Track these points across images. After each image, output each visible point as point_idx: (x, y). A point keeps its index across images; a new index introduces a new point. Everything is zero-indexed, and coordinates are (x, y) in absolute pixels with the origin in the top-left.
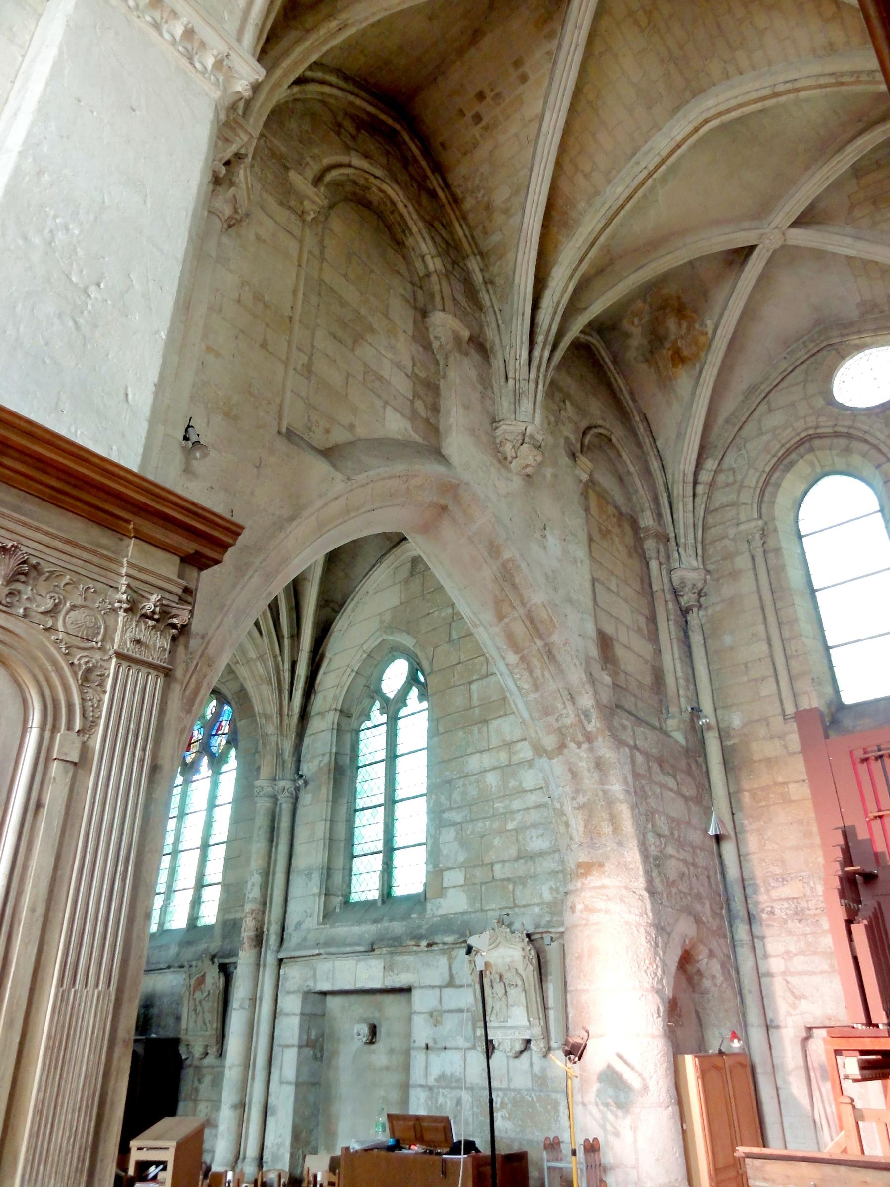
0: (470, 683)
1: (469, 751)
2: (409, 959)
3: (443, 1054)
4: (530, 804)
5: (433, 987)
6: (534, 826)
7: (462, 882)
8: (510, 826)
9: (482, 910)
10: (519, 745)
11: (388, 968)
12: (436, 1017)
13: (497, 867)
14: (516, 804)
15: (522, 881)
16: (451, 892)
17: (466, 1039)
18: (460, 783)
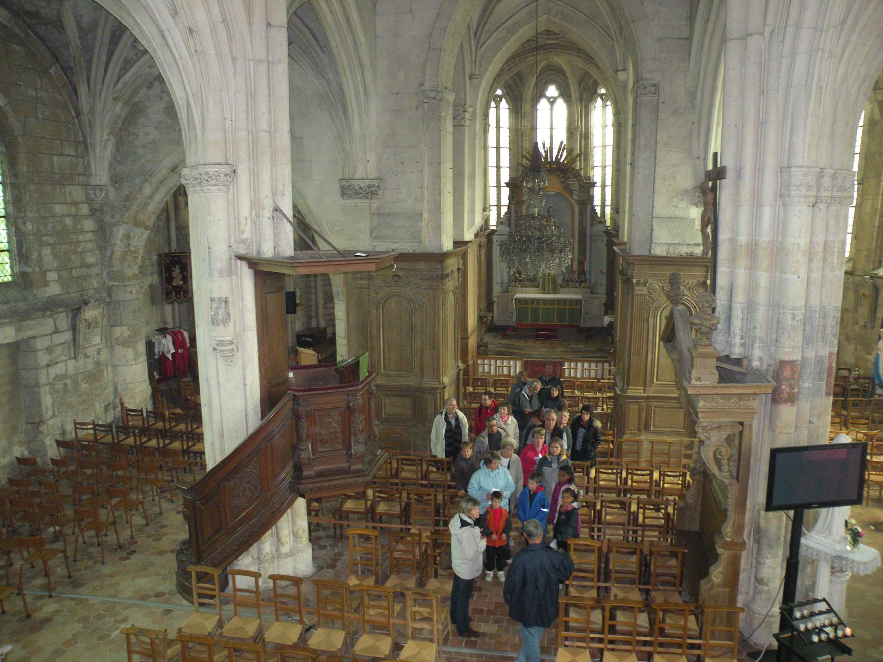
0: (53, 155)
1: (55, 201)
2: (31, 322)
3: (56, 366)
4: (87, 239)
5: (47, 335)
6: (90, 250)
7: (57, 278)
8: (79, 249)
9: (68, 293)
10: (81, 205)
11: (19, 330)
12: (49, 350)
13: (74, 270)
14: (81, 238)
15: (85, 278)
16: (52, 283)
17: (66, 356)
18: (51, 220)
